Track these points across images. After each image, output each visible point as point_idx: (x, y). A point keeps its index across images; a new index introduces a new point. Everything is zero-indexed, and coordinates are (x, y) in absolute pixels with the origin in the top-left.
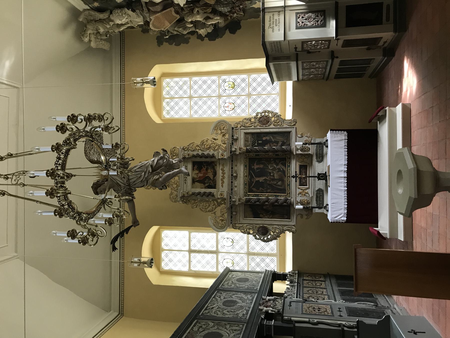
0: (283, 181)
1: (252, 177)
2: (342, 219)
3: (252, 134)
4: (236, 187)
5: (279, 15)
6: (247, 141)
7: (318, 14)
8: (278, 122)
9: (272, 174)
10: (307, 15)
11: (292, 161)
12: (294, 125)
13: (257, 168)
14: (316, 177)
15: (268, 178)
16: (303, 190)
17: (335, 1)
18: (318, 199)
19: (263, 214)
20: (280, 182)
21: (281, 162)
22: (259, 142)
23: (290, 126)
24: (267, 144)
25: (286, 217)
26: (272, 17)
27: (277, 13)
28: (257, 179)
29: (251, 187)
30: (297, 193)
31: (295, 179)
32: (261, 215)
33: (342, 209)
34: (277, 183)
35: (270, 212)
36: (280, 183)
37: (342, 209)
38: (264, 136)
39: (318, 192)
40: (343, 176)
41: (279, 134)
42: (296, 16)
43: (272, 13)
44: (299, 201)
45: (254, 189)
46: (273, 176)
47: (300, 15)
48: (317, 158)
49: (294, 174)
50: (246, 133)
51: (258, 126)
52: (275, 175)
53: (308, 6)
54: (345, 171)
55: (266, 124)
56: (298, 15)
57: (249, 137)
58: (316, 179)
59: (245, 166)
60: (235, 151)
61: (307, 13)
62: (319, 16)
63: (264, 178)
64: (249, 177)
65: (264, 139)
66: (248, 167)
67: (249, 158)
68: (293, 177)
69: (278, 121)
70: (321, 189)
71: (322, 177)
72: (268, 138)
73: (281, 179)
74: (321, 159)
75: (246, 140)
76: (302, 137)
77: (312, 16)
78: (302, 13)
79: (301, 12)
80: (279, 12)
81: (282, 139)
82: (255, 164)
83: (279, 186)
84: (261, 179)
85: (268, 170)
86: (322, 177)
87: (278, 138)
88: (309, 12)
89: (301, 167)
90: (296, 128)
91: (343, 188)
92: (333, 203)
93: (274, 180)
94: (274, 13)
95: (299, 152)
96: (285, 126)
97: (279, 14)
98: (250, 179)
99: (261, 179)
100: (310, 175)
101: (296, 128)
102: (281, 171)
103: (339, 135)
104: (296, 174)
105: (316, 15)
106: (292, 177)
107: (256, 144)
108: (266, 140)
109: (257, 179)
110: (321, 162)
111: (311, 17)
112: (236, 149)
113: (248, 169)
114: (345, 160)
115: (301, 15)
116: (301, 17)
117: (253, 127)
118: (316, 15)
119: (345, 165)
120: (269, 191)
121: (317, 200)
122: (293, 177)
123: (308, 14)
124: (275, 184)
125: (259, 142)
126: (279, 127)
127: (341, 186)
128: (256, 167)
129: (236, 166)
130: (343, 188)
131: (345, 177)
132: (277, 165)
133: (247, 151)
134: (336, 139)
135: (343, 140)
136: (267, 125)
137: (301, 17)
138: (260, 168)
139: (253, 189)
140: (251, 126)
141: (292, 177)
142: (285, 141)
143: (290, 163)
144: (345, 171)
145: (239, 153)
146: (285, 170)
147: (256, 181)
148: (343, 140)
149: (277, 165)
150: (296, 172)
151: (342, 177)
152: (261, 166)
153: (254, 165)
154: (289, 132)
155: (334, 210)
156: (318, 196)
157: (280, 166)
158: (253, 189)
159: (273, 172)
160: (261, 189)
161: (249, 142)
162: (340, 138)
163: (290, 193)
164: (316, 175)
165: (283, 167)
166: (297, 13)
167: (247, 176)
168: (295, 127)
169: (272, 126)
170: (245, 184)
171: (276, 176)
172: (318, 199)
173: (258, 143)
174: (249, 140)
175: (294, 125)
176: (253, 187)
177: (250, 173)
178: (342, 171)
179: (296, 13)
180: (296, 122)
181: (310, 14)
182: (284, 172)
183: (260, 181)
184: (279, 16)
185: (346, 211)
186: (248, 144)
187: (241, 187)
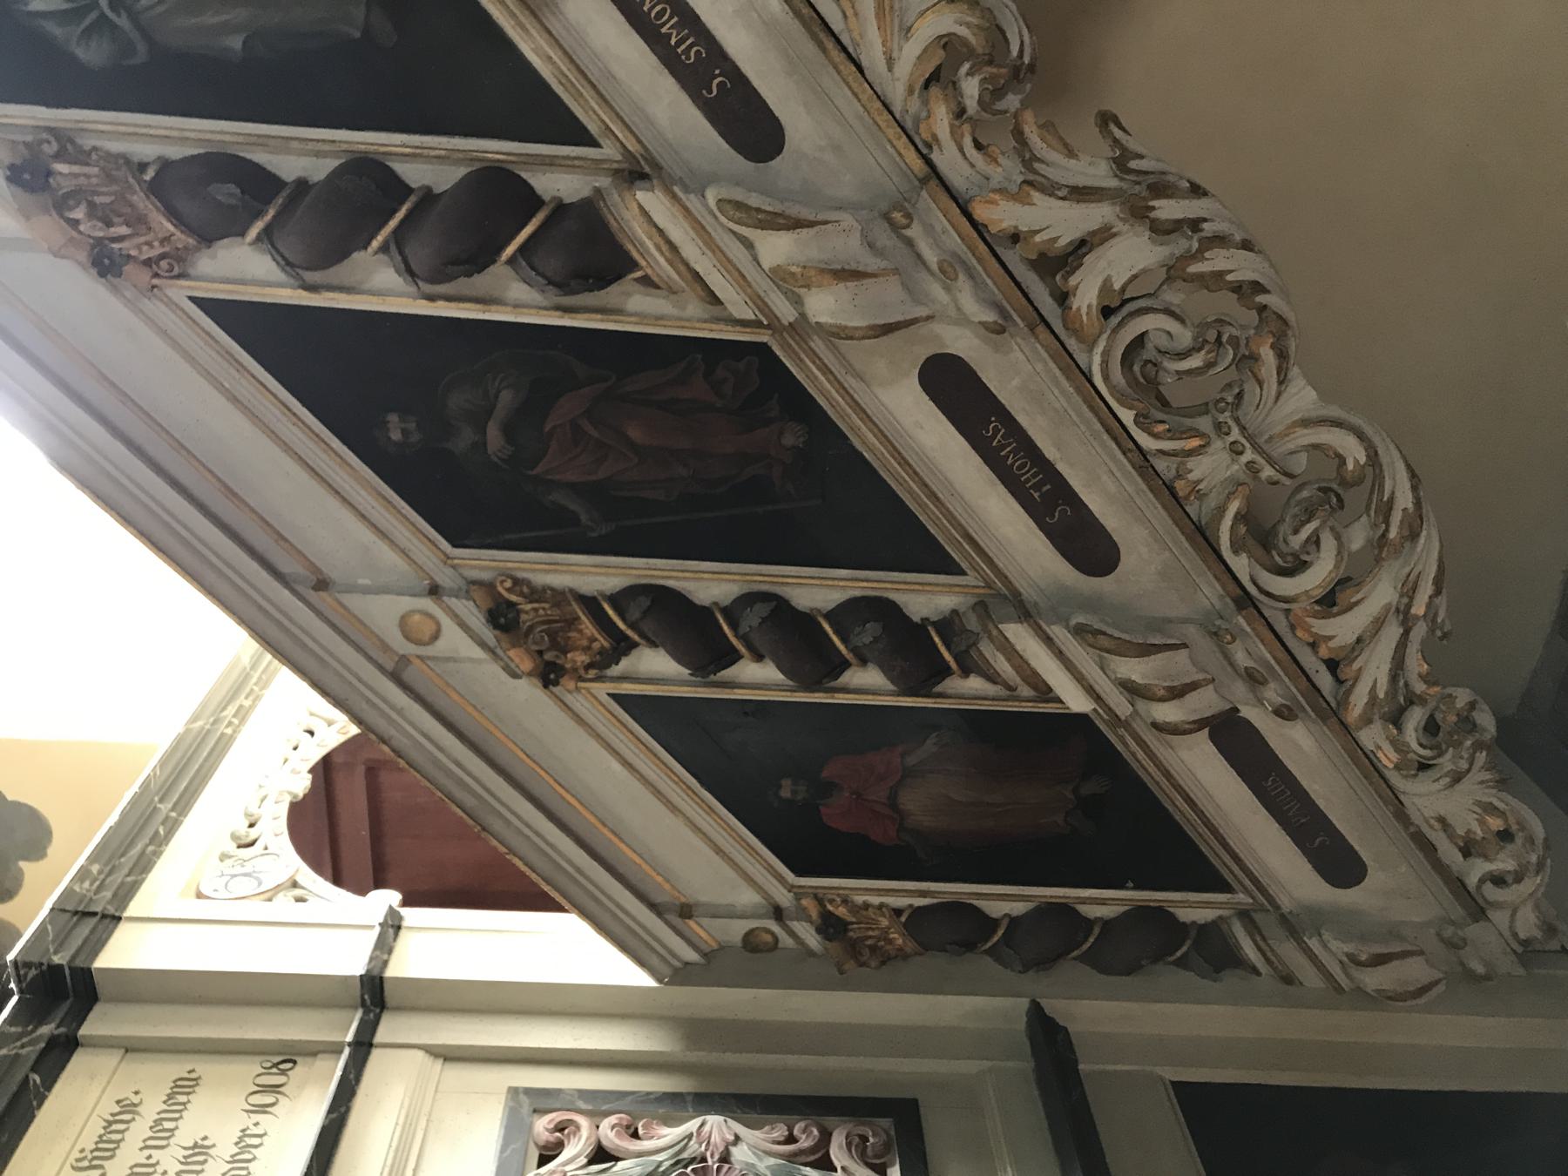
5: (269, 1099)
7: (826, 1137)
10: (670, 1134)
17: (1024, 1003)
26: (152, 1106)
27: (249, 1070)
42: (514, 1127)
43: (177, 1068)
47: (560, 1128)
53: (696, 1030)
56: (542, 1126)
61: (674, 1106)
62: (838, 1154)
77: (740, 1154)
78: (598, 1103)
79: (584, 1094)
80: (287, 1056)
88: (705, 1102)
94: (206, 1068)
97: (275, 1089)
105: (791, 1139)
111: (725, 1158)
115: (583, 1121)
116: (576, 1148)
118: (791, 1139)
123: (692, 1125)
137: (576, 1148)
166: (528, 1092)
179: (514, 1092)
181: (717, 1126)
184: (263, 1109)
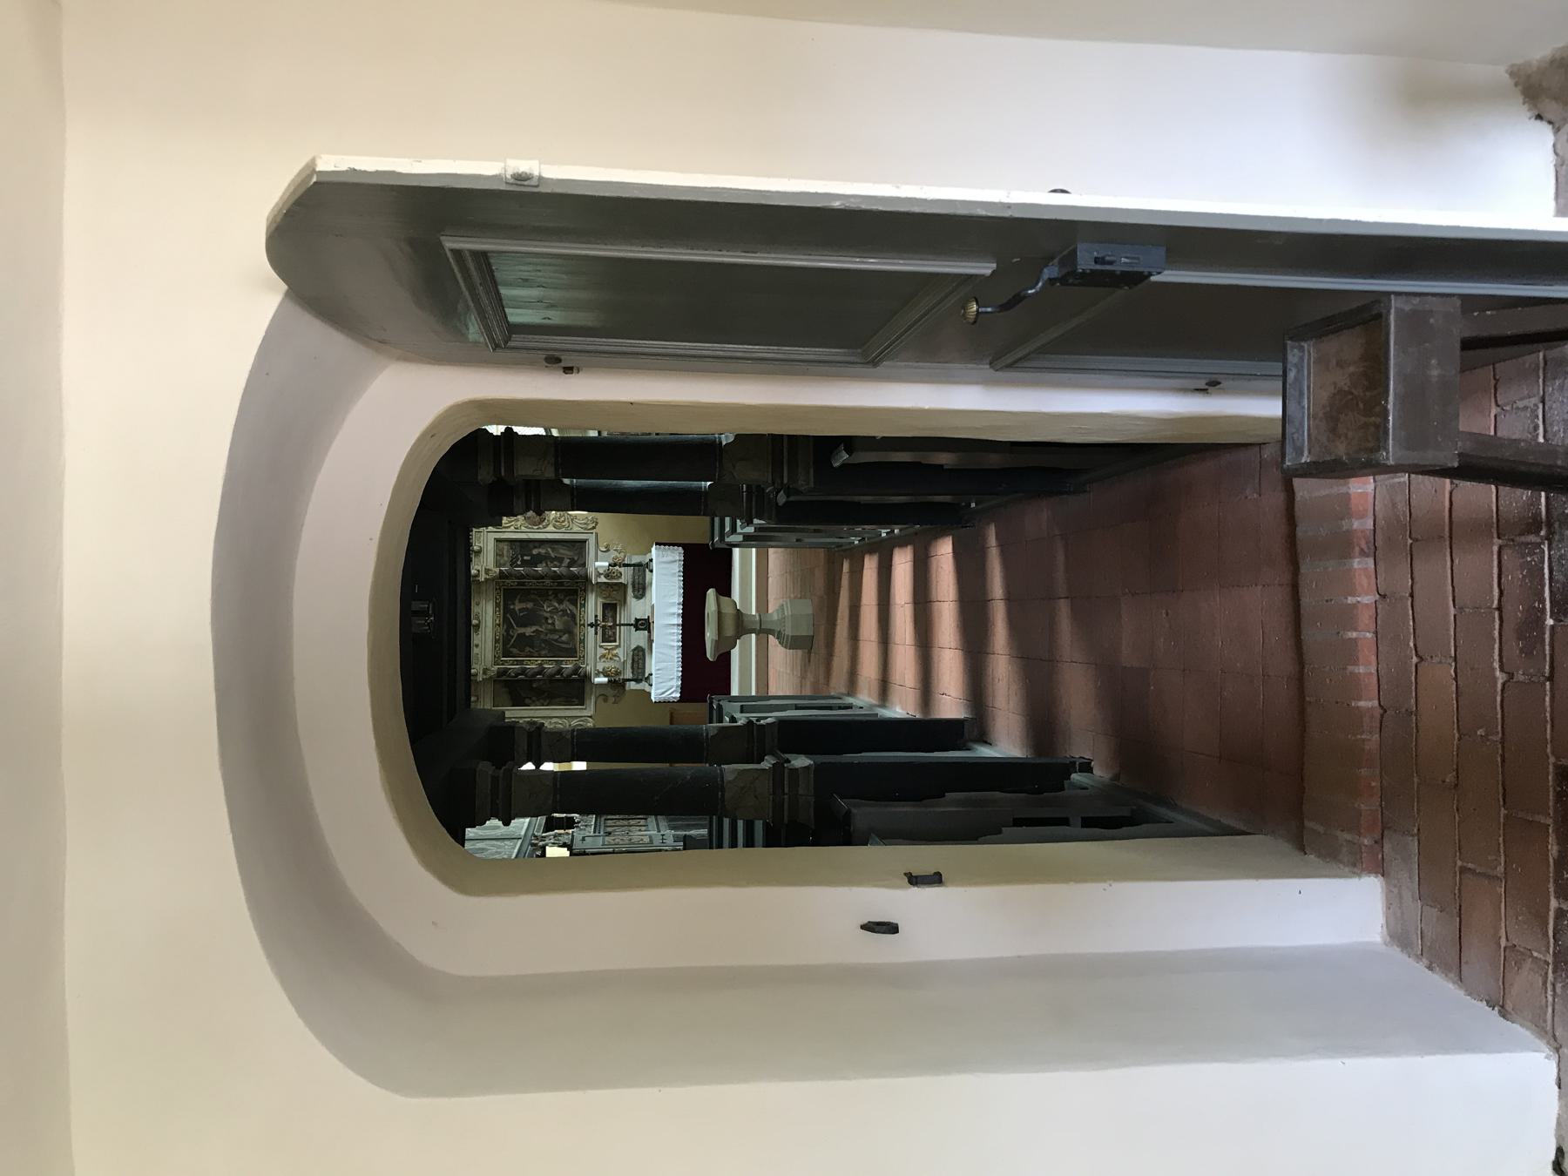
0: (570, 632)
1: (510, 626)
2: (674, 695)
3: (512, 541)
4: (477, 646)
6: (500, 555)
8: (563, 522)
9: (550, 621)
11: (590, 595)
12: (594, 528)
13: (519, 610)
14: (632, 625)
15: (541, 627)
16: (609, 650)
18: (635, 665)
19: (530, 698)
20: (566, 635)
21: (567, 598)
22: (525, 558)
23: (586, 529)
24: (541, 563)
25: (576, 701)
28: (521, 630)
29: (509, 646)
30: (598, 657)
31: (593, 629)
32: (527, 701)
33: (673, 679)
34: (560, 637)
35: (546, 694)
36: (564, 638)
37: (673, 679)
38: (535, 547)
39: (636, 652)
40: (676, 623)
41: (565, 544)
44: (601, 670)
45: (515, 651)
46: (553, 624)
48: (633, 591)
49: (592, 620)
50: (498, 541)
51: (523, 528)
52: (557, 622)
54: (679, 615)
55: (540, 524)
57: (506, 547)
58: (633, 629)
59: (497, 605)
60: (477, 576)
63: (534, 628)
64: (505, 627)
65: (535, 552)
66: (502, 607)
67: (504, 589)
68: (591, 625)
69: (563, 519)
70: (641, 647)
71: (642, 624)
72: (543, 551)
73: (569, 631)
74: (640, 593)
75: (498, 554)
76: (608, 550)
81: (568, 553)
82: (517, 602)
83: (563, 642)
84: (529, 631)
85: (541, 613)
86: (642, 624)
87: (562, 551)
89: (605, 606)
90: (597, 534)
91: (676, 644)
92: (658, 670)
93: (554, 631)
95: (603, 579)
96: (576, 529)
98: (507, 631)
99: (529, 631)
100: (622, 622)
101: (597, 534)
102: (568, 615)
103: (669, 553)
104: (596, 621)
106: (589, 625)
107: (519, 563)
108: (539, 554)
109: (521, 630)
110: (641, 598)
112: (478, 571)
113: (502, 611)
114: (679, 596)
117: (512, 528)
119: (679, 604)
120: (543, 653)
121: (632, 668)
122: (591, 625)
124: (556, 641)
125: (525, 558)
126: (563, 530)
127: (673, 641)
128: (518, 606)
129: (478, 604)
130: (676, 644)
131: (678, 625)
132: (560, 602)
133: (502, 575)
134: (665, 559)
135: (675, 561)
136: (541, 526)
138: (528, 609)
139: (511, 649)
140: (509, 527)
141: (589, 625)
142: (576, 558)
143: (585, 600)
144: (679, 615)
145: (485, 579)
146: (575, 611)
147: (518, 634)
148: (675, 561)
149: (560, 602)
150: (596, 616)
151: (674, 625)
152: (530, 605)
153: (514, 604)
154: (584, 542)
155: (661, 680)
156: (636, 659)
157: (566, 605)
158: (511, 649)
159: (552, 618)
160: (528, 649)
161: (506, 558)
162: (670, 558)
163: (584, 657)
164: (633, 622)
165: (572, 607)
167: (499, 625)
168: (594, 531)
169: (551, 528)
170: (497, 641)
171: (558, 625)
172: (635, 665)
173: (523, 561)
174: (505, 552)
175: (594, 528)
176: (513, 646)
177: (505, 619)
178: (674, 614)
180: (597, 523)
182: (573, 616)
183: (527, 634)
185: (680, 683)
186: (502, 562)
187: (487, 646)
